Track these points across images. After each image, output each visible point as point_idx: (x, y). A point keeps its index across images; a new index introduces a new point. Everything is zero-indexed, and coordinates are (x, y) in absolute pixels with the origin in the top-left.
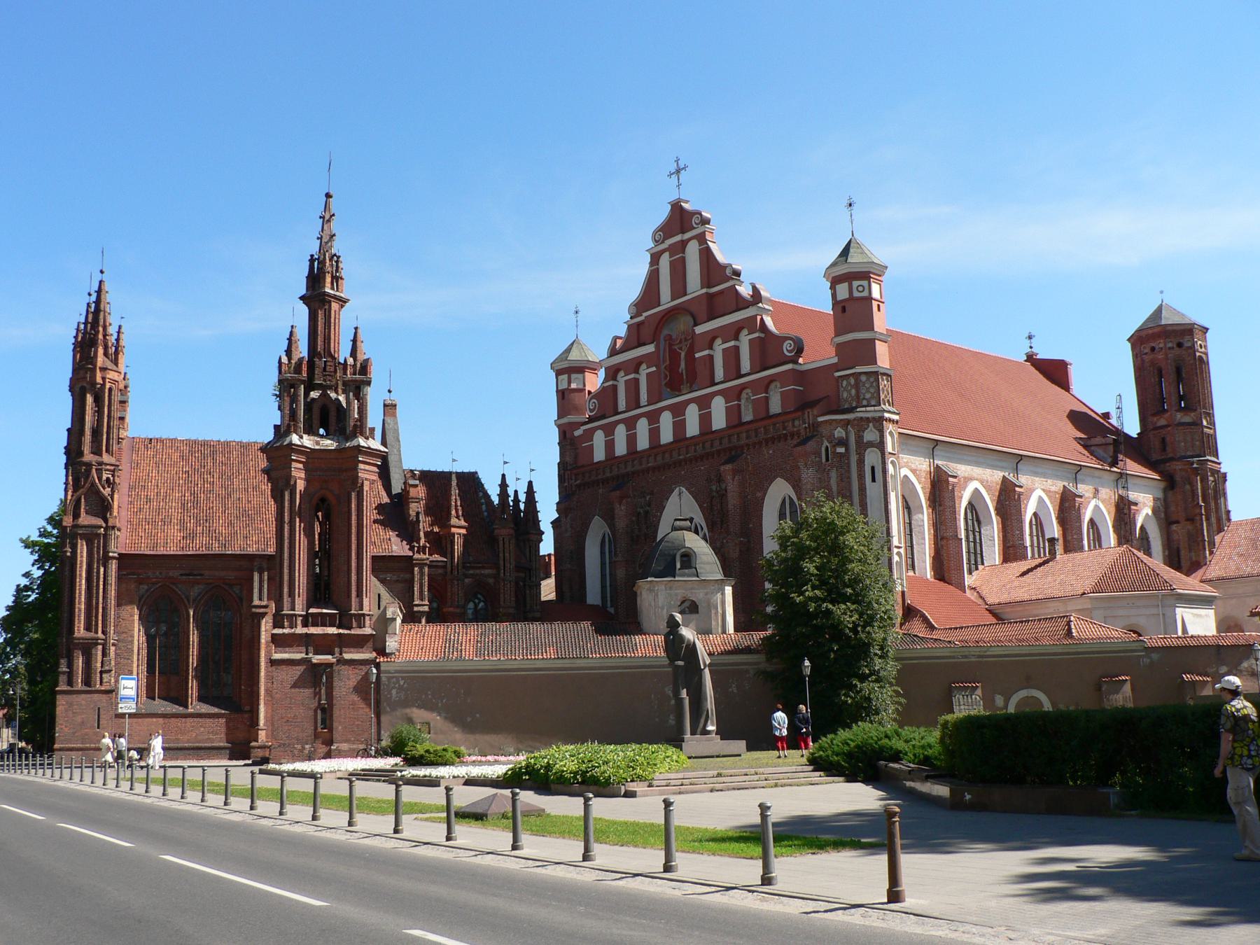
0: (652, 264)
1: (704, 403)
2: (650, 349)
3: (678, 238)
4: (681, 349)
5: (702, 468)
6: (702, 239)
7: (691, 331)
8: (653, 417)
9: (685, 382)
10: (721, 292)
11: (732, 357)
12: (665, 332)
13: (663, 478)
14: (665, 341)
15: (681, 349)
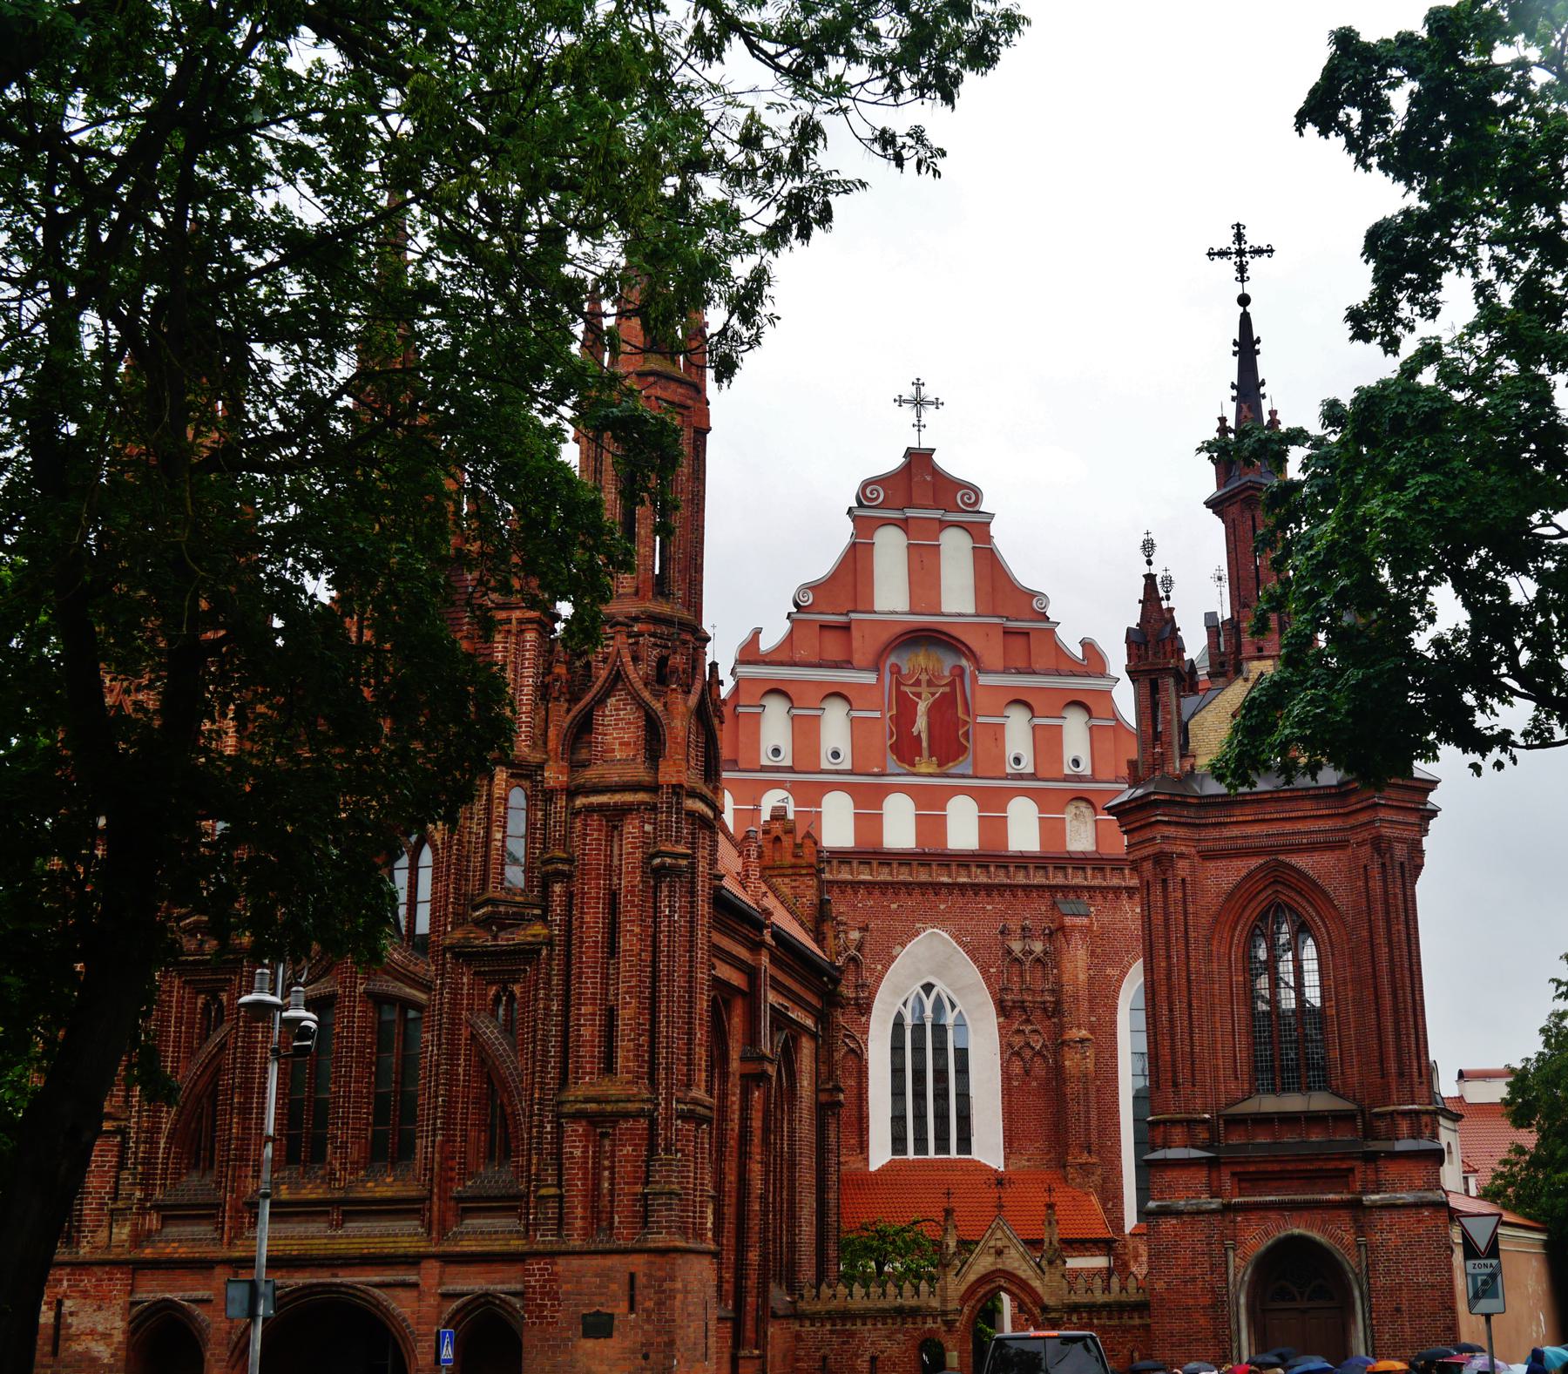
0: (855, 535)
1: (992, 803)
2: (869, 678)
3: (937, 514)
4: (919, 695)
5: (989, 907)
6: (979, 531)
7: (947, 673)
8: (868, 799)
9: (925, 753)
10: (1025, 634)
11: (1047, 741)
12: (893, 659)
13: (894, 906)
14: (892, 673)
15: (919, 695)
